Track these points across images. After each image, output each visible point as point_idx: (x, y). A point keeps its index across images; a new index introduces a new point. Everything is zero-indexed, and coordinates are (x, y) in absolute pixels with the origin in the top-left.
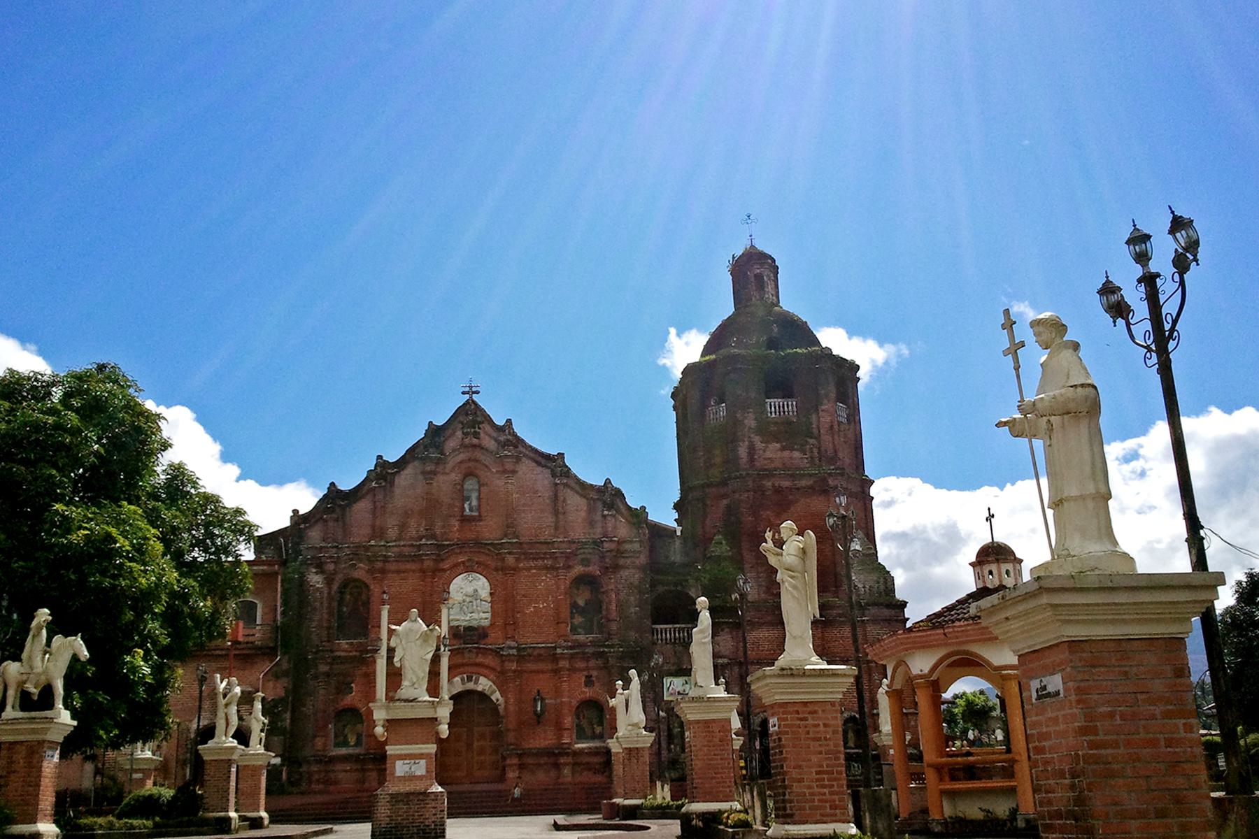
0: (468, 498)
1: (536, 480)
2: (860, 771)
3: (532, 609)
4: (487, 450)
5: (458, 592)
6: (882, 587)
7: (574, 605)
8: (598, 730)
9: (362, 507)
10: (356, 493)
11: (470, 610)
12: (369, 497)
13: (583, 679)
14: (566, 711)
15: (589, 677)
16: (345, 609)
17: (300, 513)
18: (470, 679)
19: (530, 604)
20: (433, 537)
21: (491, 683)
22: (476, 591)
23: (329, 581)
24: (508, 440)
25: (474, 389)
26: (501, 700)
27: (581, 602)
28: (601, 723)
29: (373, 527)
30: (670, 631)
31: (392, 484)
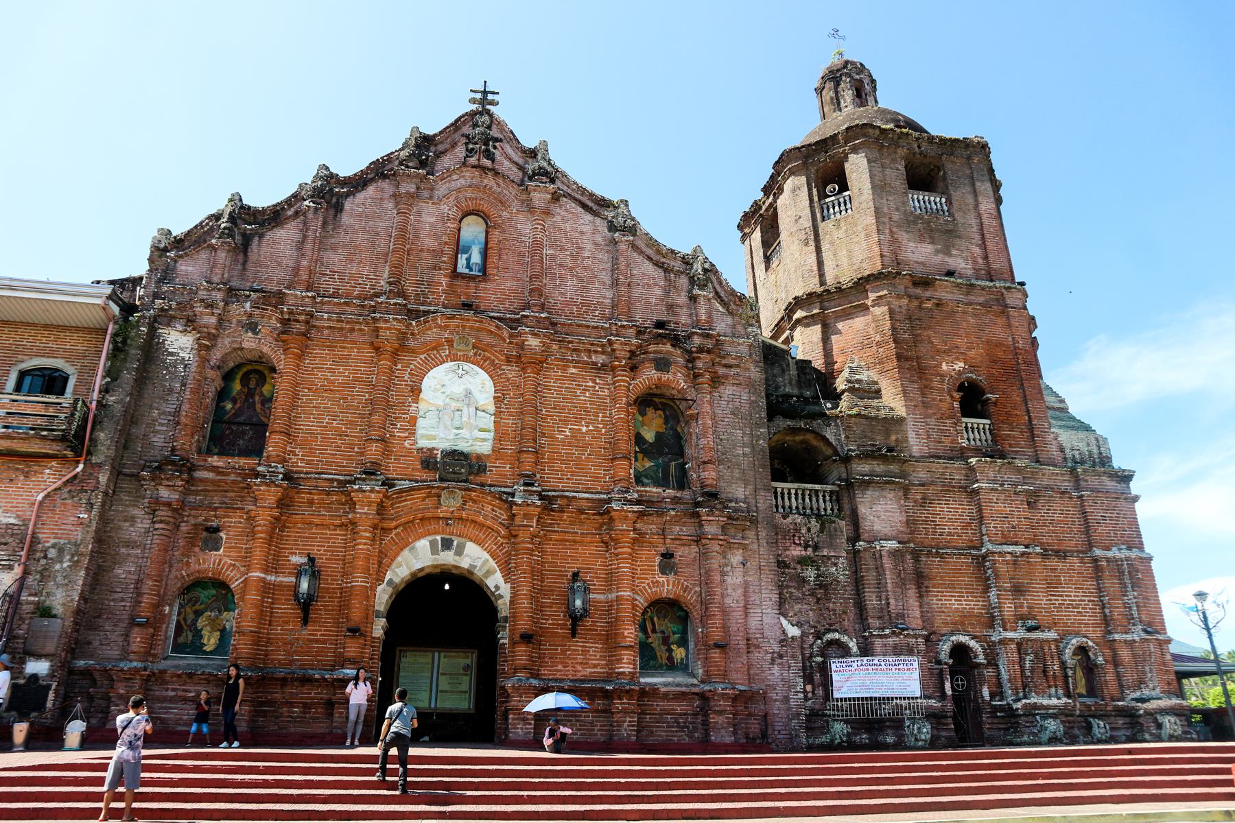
0: (467, 250)
1: (582, 233)
3: (568, 433)
4: (486, 243)
5: (436, 390)
6: (1095, 451)
7: (639, 439)
8: (679, 653)
9: (282, 239)
10: (275, 216)
11: (457, 423)
12: (298, 222)
13: (658, 559)
14: (626, 614)
15: (667, 556)
16: (229, 406)
17: (174, 234)
18: (447, 544)
19: (566, 421)
20: (402, 294)
21: (487, 556)
22: (468, 394)
23: (203, 349)
24: (540, 168)
25: (490, 97)
26: (505, 590)
27: (649, 436)
28: (683, 643)
29: (296, 269)
30: (796, 494)
31: (339, 208)
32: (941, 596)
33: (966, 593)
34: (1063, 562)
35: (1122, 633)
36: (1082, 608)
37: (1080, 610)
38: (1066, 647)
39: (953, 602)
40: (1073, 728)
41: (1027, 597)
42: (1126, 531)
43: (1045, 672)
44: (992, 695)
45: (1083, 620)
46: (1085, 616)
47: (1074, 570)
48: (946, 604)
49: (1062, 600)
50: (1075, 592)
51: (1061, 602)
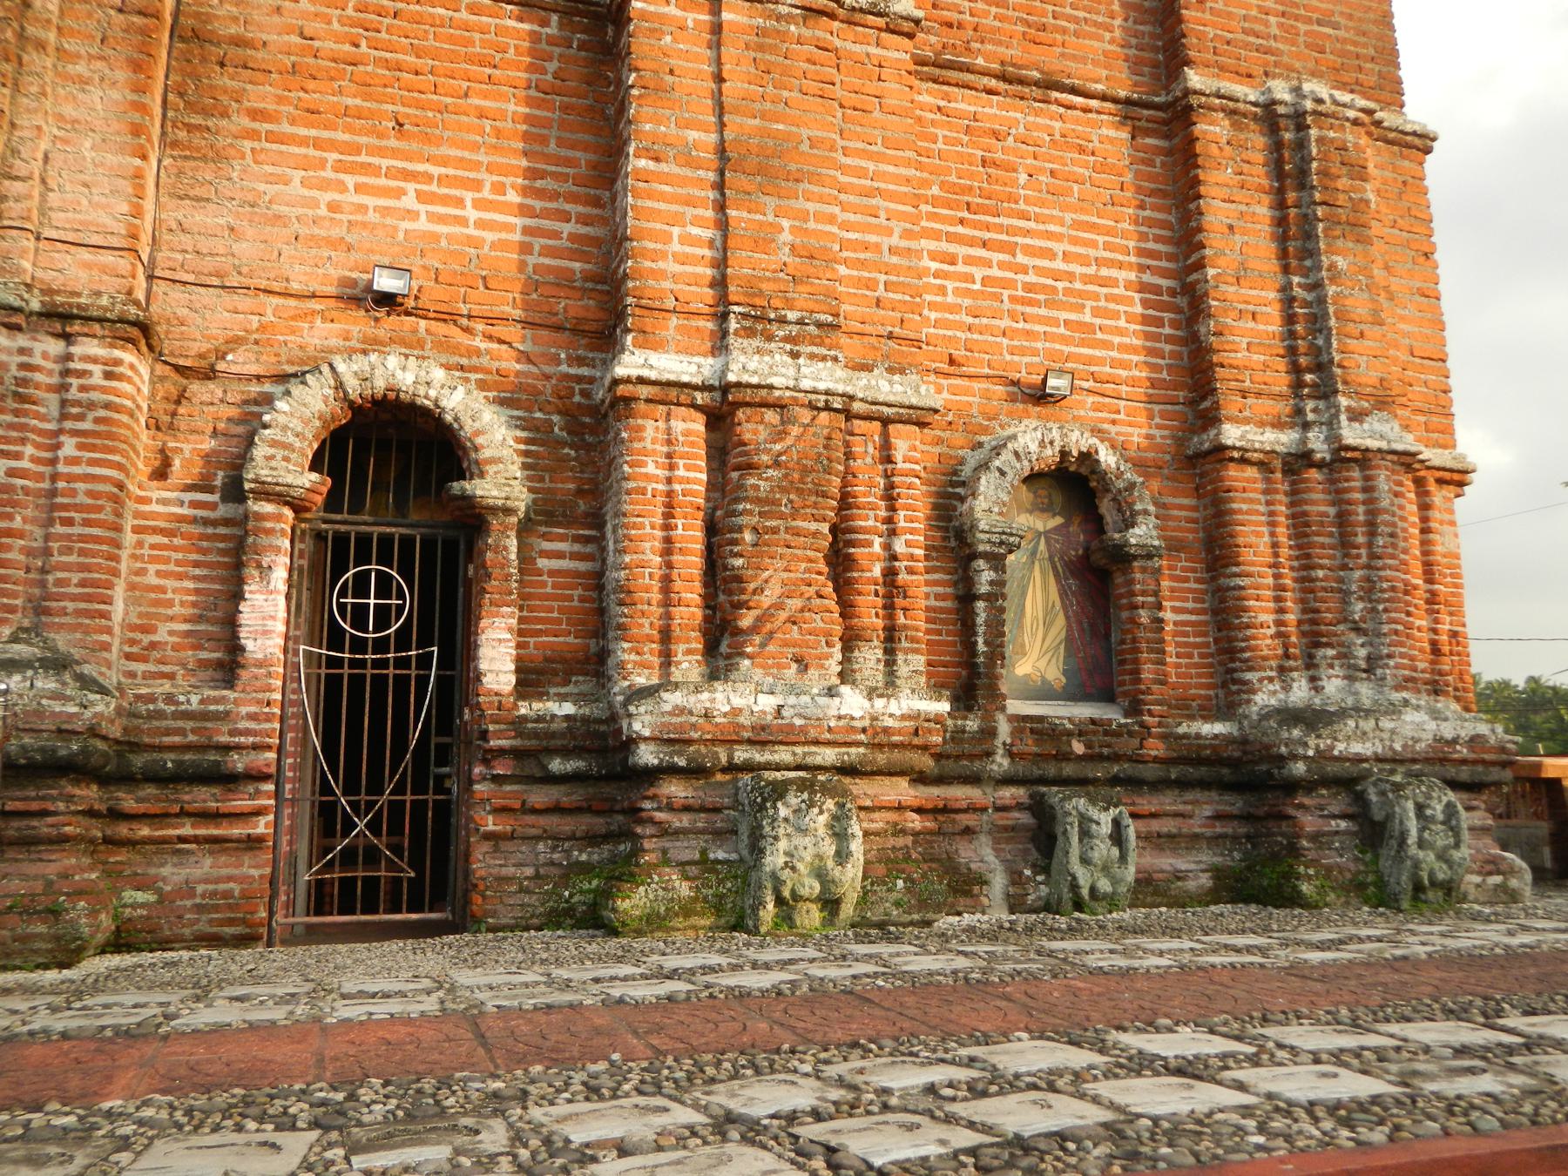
2: (1130, 873)
32: (340, 167)
33: (490, 169)
34: (1037, 113)
35: (1262, 424)
36: (1096, 312)
37: (1087, 317)
38: (984, 466)
39: (409, 202)
40: (968, 832)
41: (800, 204)
42: (1336, 26)
43: (840, 562)
44: (530, 679)
45: (1090, 361)
46: (1107, 345)
47: (1082, 150)
48: (362, 208)
49: (1001, 265)
50: (1075, 241)
51: (995, 272)
